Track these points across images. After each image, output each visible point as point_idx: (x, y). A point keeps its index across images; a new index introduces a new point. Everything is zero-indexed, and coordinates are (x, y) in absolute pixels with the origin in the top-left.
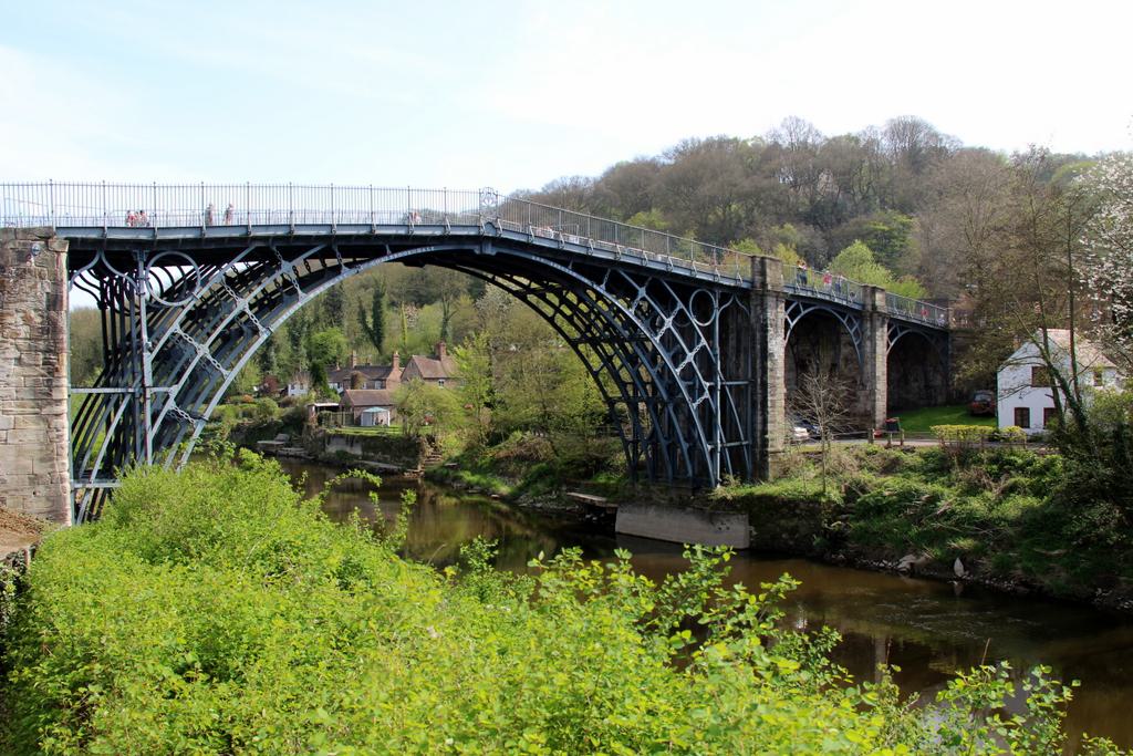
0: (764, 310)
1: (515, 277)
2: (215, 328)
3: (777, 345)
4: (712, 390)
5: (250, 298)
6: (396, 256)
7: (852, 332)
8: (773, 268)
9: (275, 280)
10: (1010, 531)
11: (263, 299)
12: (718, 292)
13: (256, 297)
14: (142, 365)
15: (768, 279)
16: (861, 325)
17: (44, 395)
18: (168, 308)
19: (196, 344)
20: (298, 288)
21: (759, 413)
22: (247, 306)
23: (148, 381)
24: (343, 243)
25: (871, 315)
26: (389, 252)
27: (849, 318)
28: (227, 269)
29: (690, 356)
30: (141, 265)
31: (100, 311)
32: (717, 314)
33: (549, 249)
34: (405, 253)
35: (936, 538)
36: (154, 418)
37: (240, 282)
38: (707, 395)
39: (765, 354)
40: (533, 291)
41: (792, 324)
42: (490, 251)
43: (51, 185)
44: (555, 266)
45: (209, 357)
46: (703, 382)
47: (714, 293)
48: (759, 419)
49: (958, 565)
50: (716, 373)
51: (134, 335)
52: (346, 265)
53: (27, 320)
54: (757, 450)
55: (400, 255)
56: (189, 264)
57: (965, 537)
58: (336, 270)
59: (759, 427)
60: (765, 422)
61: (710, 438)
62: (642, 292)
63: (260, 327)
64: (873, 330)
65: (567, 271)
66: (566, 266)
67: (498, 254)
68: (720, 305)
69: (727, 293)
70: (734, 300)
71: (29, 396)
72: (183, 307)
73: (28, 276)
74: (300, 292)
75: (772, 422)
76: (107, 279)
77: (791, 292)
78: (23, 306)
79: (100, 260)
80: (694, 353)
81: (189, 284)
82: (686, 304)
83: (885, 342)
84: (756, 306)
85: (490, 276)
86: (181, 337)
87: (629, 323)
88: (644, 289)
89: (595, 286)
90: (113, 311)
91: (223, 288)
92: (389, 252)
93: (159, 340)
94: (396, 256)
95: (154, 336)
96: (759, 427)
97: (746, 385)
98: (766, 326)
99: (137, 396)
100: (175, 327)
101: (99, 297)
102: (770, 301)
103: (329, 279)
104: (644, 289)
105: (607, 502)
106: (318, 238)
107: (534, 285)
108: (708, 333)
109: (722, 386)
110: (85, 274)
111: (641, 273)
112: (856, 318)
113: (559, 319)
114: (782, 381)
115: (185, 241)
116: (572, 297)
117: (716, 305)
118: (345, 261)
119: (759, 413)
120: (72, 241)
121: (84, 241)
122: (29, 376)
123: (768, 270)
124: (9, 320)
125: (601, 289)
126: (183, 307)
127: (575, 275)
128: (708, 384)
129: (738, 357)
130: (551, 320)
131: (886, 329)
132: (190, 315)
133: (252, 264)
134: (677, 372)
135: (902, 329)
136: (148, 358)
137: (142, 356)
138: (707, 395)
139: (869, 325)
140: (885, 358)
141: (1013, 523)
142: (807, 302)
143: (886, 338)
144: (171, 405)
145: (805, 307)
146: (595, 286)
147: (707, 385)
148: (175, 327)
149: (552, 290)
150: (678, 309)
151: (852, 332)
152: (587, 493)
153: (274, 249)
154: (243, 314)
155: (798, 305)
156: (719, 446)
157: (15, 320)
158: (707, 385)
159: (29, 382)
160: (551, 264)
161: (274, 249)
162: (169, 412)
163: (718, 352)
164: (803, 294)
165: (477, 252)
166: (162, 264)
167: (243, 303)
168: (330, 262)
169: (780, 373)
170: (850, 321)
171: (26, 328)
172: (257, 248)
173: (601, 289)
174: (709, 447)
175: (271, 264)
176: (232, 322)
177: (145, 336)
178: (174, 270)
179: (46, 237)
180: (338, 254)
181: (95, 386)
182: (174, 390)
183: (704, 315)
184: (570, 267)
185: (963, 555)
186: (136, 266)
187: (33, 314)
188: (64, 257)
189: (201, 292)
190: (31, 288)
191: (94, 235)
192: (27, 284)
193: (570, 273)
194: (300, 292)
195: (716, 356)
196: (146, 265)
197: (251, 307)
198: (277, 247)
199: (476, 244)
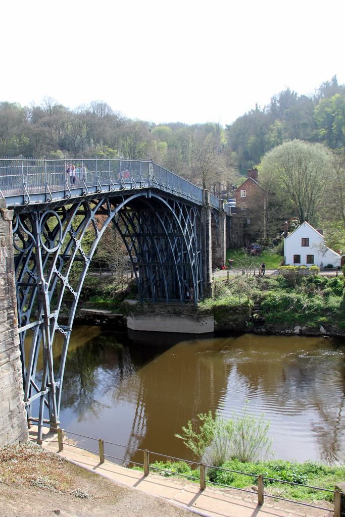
10: (339, 312)
24: (109, 196)
26: (123, 200)
35: (310, 317)
49: (322, 329)
54: (205, 283)
57: (323, 316)
59: (206, 272)
66: (166, 200)
84: (204, 214)
92: (123, 200)
96: (206, 272)
105: (112, 313)
127: (168, 206)
141: (339, 309)
152: (92, 308)
165: (147, 197)
185: (323, 323)
199: (146, 192)
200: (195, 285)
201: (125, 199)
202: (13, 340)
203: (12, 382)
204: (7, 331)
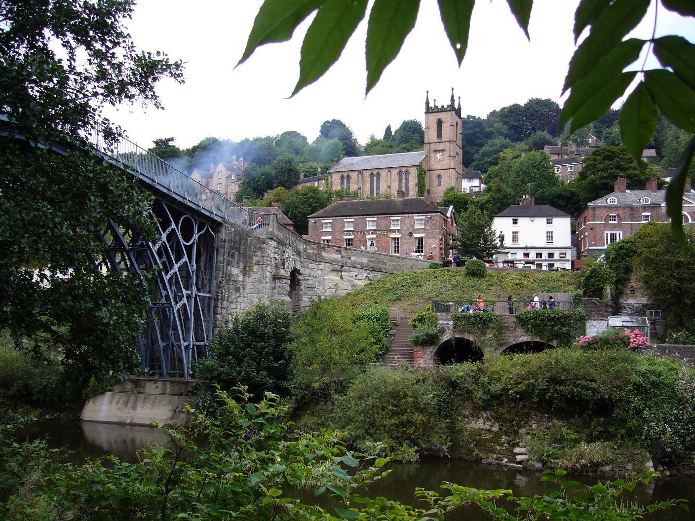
4: (189, 297)
29: (176, 267)
32: (196, 237)
38: (185, 300)
46: (184, 290)
47: (195, 220)
68: (198, 232)
70: (207, 228)
82: (177, 226)
97: (210, 298)
109: (196, 295)
117: (196, 230)
138: (185, 300)
147: (185, 292)
158: (185, 292)
163: (195, 268)
174: (186, 344)
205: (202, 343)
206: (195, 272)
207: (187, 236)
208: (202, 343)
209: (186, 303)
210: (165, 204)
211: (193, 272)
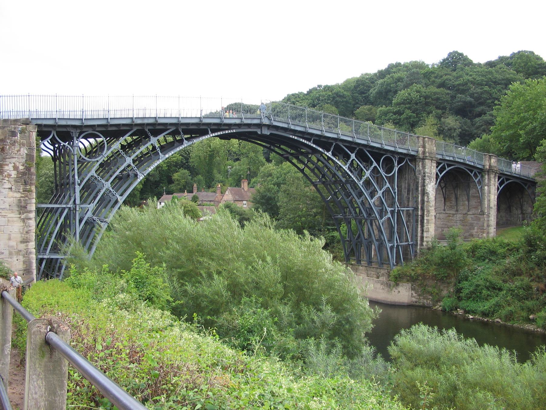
0: (424, 167)
1: (282, 146)
2: (114, 172)
3: (431, 187)
4: (392, 212)
5: (134, 156)
6: (214, 135)
7: (476, 181)
8: (430, 143)
9: (147, 147)
11: (141, 157)
12: (397, 157)
13: (137, 156)
14: (75, 193)
15: (427, 150)
16: (482, 177)
17: (22, 208)
18: (89, 162)
19: (103, 181)
20: (159, 152)
21: (419, 226)
22: (132, 161)
23: (78, 201)
25: (488, 172)
26: (210, 132)
27: (475, 173)
28: (122, 140)
29: (380, 193)
30: (75, 139)
31: (53, 163)
32: (396, 169)
33: (300, 132)
34: (219, 133)
36: (80, 221)
37: (127, 148)
39: (424, 193)
40: (292, 154)
41: (441, 176)
42: (266, 132)
43: (29, 96)
44: (303, 141)
45: (111, 189)
46: (387, 208)
47: (394, 157)
48: (419, 229)
50: (395, 203)
51: (71, 177)
52: (186, 139)
53: (15, 168)
55: (216, 134)
56: (101, 137)
58: (181, 142)
59: (419, 235)
60: (422, 231)
61: (390, 240)
62: (353, 156)
63: (138, 173)
64: (489, 179)
65: (310, 144)
66: (309, 140)
67: (271, 134)
68: (398, 165)
69: (402, 157)
70: (407, 162)
71: (15, 208)
72: (98, 161)
73: (17, 144)
74: (160, 154)
75: (426, 232)
76: (57, 146)
77: (440, 157)
78: (14, 160)
79: (54, 135)
80: (382, 191)
81: (101, 147)
82: (379, 166)
83: (496, 187)
85: (268, 145)
86: (96, 178)
87: (345, 174)
88: (354, 154)
89: (326, 153)
90: (60, 162)
91: (118, 151)
92: (210, 132)
93: (83, 179)
94: (214, 135)
95: (81, 178)
96: (419, 235)
98: (425, 176)
99: (72, 209)
100: (93, 172)
101: (53, 154)
102: (428, 163)
103: (177, 147)
104: (354, 154)
106: (171, 124)
107: (292, 151)
108: (391, 180)
109: (399, 211)
110: (46, 143)
111: (352, 146)
112: (479, 173)
113: (307, 171)
114: (433, 208)
115: (99, 126)
116: (314, 159)
117: (396, 164)
118: (186, 136)
119: (419, 226)
120: (39, 126)
121: (46, 126)
122: (16, 197)
123: (426, 144)
124: (6, 168)
125: (329, 154)
126: (98, 161)
127: (314, 146)
128: (390, 209)
129: (408, 194)
130: (302, 171)
131: (497, 180)
132: (101, 165)
133: (134, 138)
134: (372, 201)
135: (507, 180)
136: (78, 189)
137: (75, 188)
138: (389, 215)
139: (486, 177)
140: (496, 197)
142: (450, 163)
143: (497, 184)
144: (89, 214)
145: (449, 166)
146: (326, 153)
147: (389, 209)
148: (93, 172)
149: (302, 154)
150: (373, 166)
151: (476, 181)
153: (147, 131)
154: (129, 166)
155: (444, 165)
156: (396, 244)
157: (9, 168)
158: (389, 209)
159: (16, 201)
160: (301, 140)
161: (147, 131)
162: (88, 218)
163: (396, 191)
164: (448, 158)
165: (259, 133)
166: (86, 138)
167: (129, 160)
168: (178, 138)
169: (432, 203)
170: (475, 174)
171: (15, 172)
172: (137, 129)
173: (329, 154)
174: (390, 245)
175: (145, 138)
176: (124, 170)
177: (76, 177)
178: (92, 140)
179: (27, 122)
180: (182, 133)
181: (50, 203)
182: (92, 207)
183: (389, 170)
184: (312, 142)
186: (73, 138)
187: (18, 164)
188: (34, 135)
189: (107, 153)
190: (18, 151)
191: (51, 123)
192: (17, 147)
193: (312, 145)
194: (160, 154)
195: (395, 193)
196: (78, 138)
197: (134, 161)
198: (149, 130)
199: (259, 128)
200: (389, 245)
201: (213, 131)
202: (27, 205)
203: (21, 231)
204: (22, 199)
205: (407, 243)
206: (396, 194)
207: (389, 170)
208: (407, 243)
209: (390, 216)
210: (367, 150)
211: (395, 193)
